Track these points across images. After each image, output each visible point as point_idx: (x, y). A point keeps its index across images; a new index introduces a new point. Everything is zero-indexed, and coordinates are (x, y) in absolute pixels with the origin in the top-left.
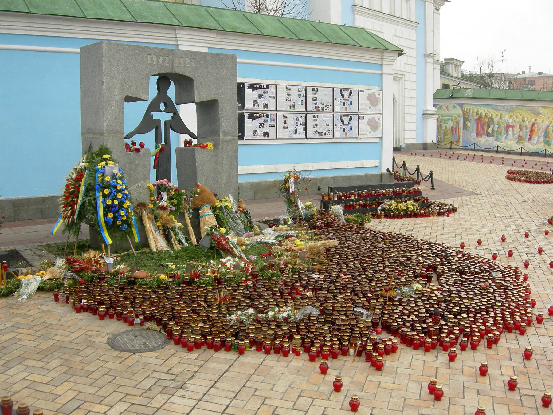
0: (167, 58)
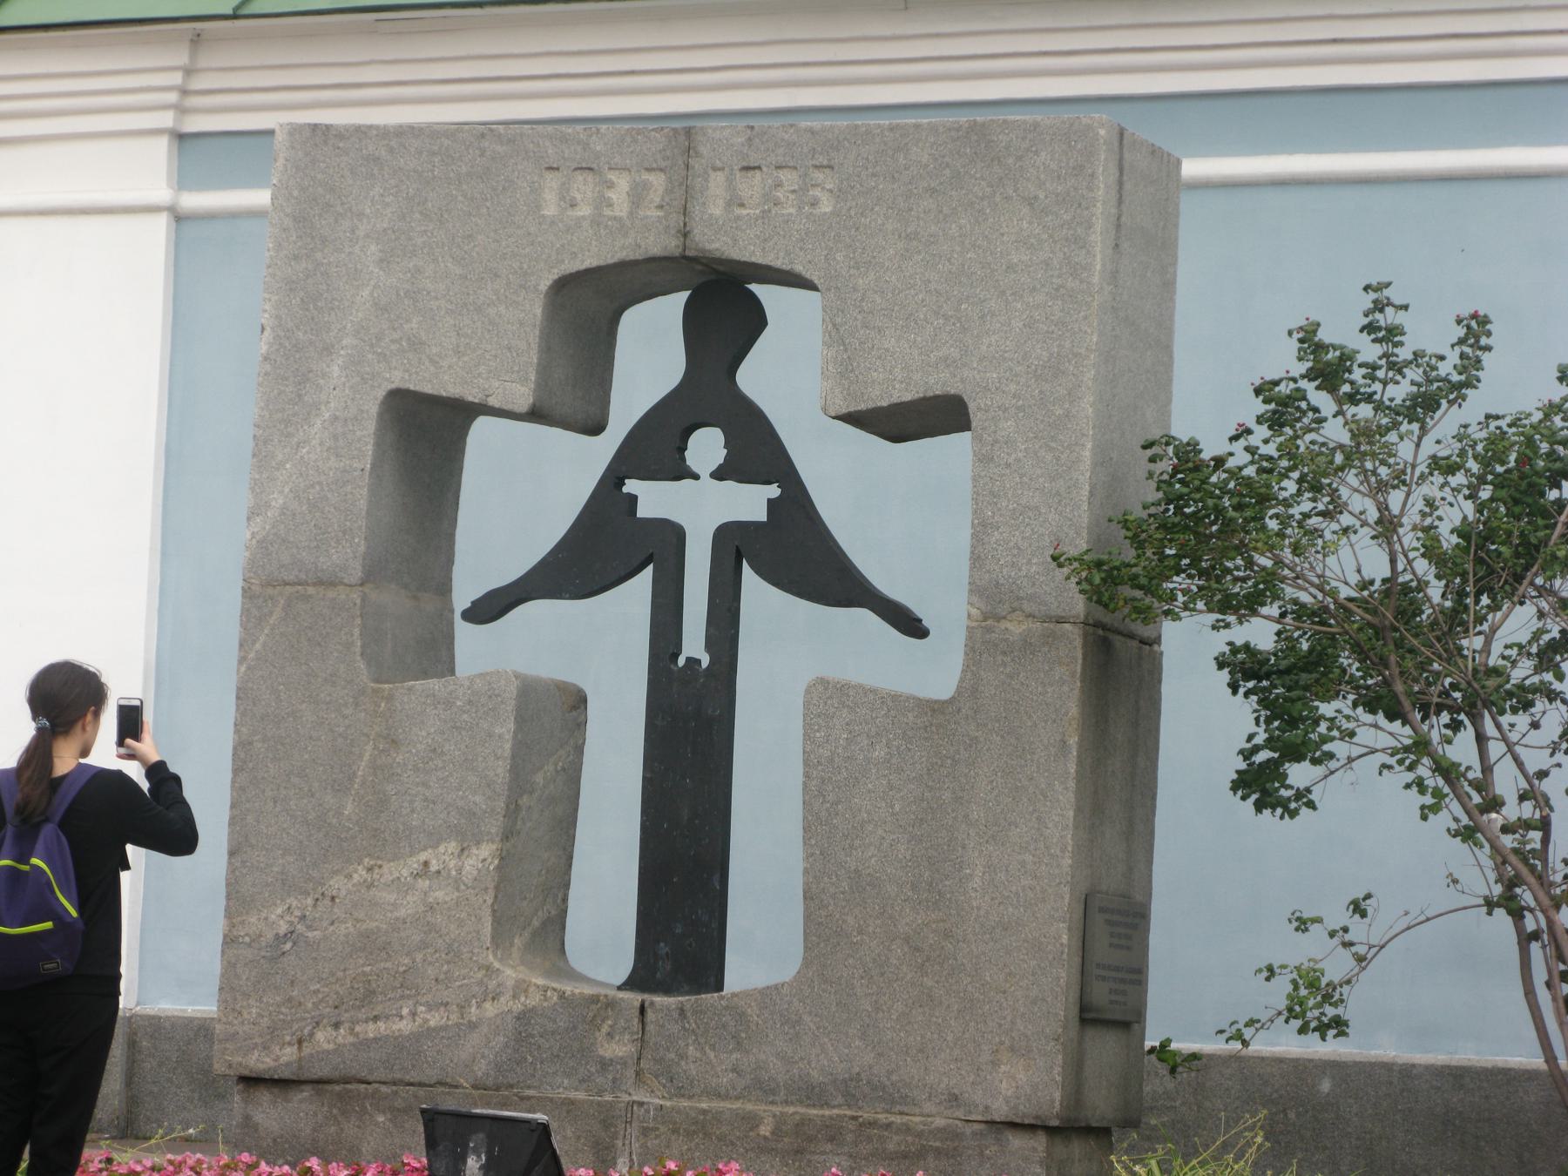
0: (657, 181)
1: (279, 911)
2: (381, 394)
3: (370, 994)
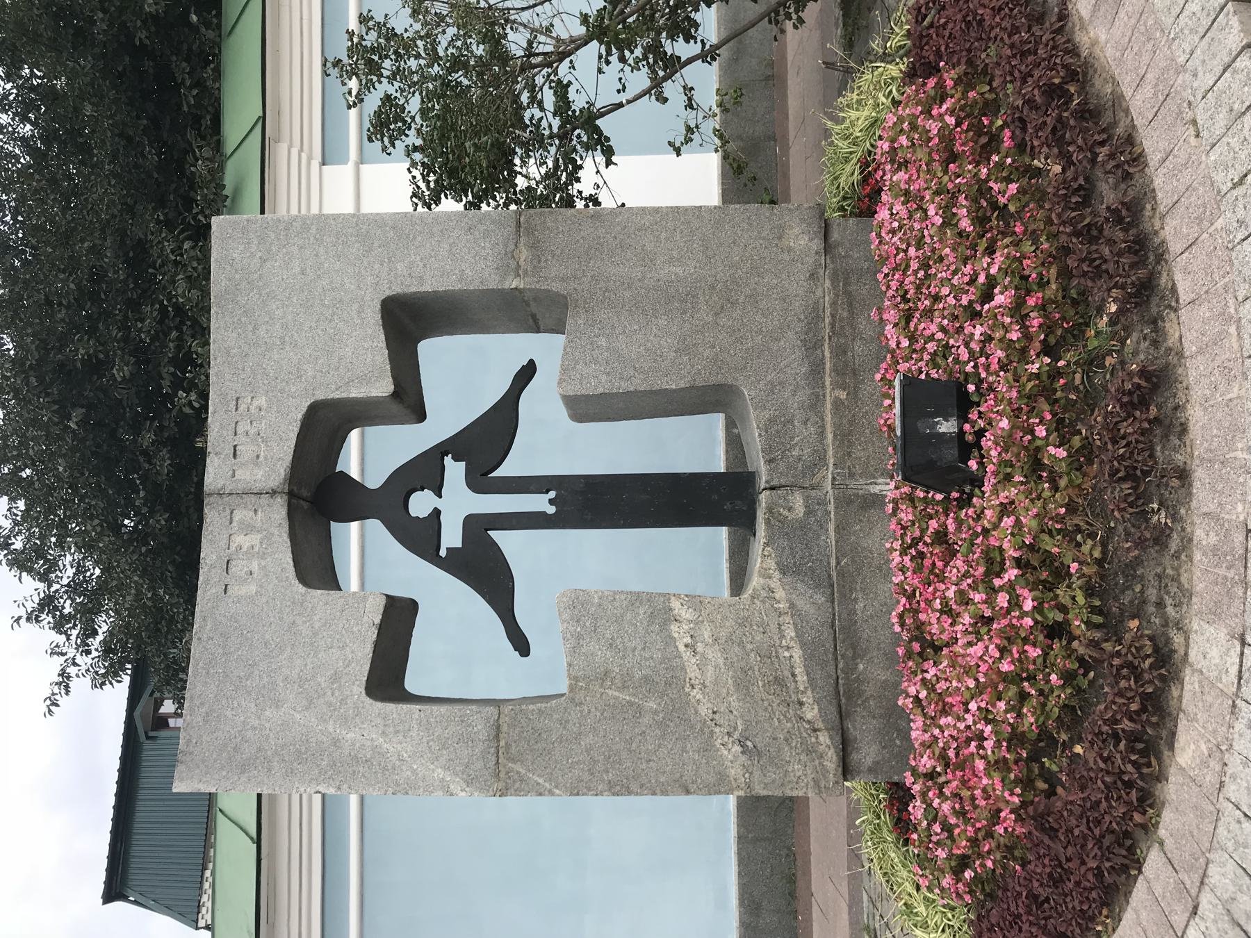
0: (238, 515)
1: (726, 752)
2: (368, 701)
3: (779, 681)
